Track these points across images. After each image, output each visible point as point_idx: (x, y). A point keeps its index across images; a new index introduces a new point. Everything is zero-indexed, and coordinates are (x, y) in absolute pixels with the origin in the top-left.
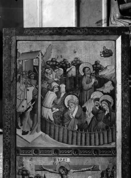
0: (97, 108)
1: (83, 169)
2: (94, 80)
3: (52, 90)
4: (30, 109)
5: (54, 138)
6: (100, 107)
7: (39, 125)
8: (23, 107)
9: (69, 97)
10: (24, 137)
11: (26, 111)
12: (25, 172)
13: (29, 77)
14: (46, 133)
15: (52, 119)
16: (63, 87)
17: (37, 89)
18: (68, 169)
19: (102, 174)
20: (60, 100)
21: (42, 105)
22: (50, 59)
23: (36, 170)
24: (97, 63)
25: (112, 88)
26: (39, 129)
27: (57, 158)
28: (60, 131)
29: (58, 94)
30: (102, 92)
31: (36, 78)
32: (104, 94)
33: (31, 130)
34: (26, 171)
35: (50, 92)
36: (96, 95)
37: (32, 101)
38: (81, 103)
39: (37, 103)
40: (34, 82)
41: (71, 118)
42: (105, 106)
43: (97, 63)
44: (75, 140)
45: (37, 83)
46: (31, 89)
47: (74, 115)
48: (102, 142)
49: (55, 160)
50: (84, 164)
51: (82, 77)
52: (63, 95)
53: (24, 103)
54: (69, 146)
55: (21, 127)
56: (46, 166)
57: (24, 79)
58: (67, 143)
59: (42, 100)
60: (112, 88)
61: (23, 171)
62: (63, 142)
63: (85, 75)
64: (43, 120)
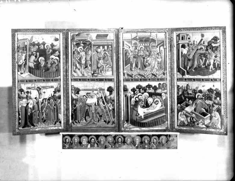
0: (53, 62)
1: (47, 88)
2: (51, 51)
3: (33, 55)
4: (24, 63)
5: (34, 75)
6: (54, 62)
7: (28, 70)
8: (21, 62)
9: (41, 58)
10: (21, 75)
11: (22, 64)
12: (22, 90)
13: (23, 50)
14: (31, 73)
15: (33, 67)
16: (38, 54)
17: (27, 54)
18: (41, 88)
19: (55, 89)
20: (37, 59)
21: (29, 61)
22: (32, 42)
23: (27, 89)
24: (52, 44)
25: (59, 54)
26: (28, 71)
27: (36, 84)
28: (38, 72)
29: (36, 57)
30: (55, 56)
31: (26, 50)
32: (56, 56)
33: (24, 72)
34: (23, 90)
35: (32, 56)
36: (52, 56)
37: (25, 60)
38: (46, 60)
39: (27, 61)
40: (25, 52)
41: (42, 66)
42: (56, 61)
43: (52, 44)
44: (43, 76)
45: (27, 52)
46: (24, 55)
47: (43, 65)
48: (55, 76)
49: (35, 84)
50: (47, 86)
51: (46, 49)
52: (38, 57)
53: (21, 61)
54: (41, 78)
55: (20, 71)
56: (31, 87)
57: (21, 51)
58: (40, 77)
59: (29, 59)
60: (59, 54)
61: (21, 89)
62: (38, 77)
63: (47, 49)
64: (29, 67)
